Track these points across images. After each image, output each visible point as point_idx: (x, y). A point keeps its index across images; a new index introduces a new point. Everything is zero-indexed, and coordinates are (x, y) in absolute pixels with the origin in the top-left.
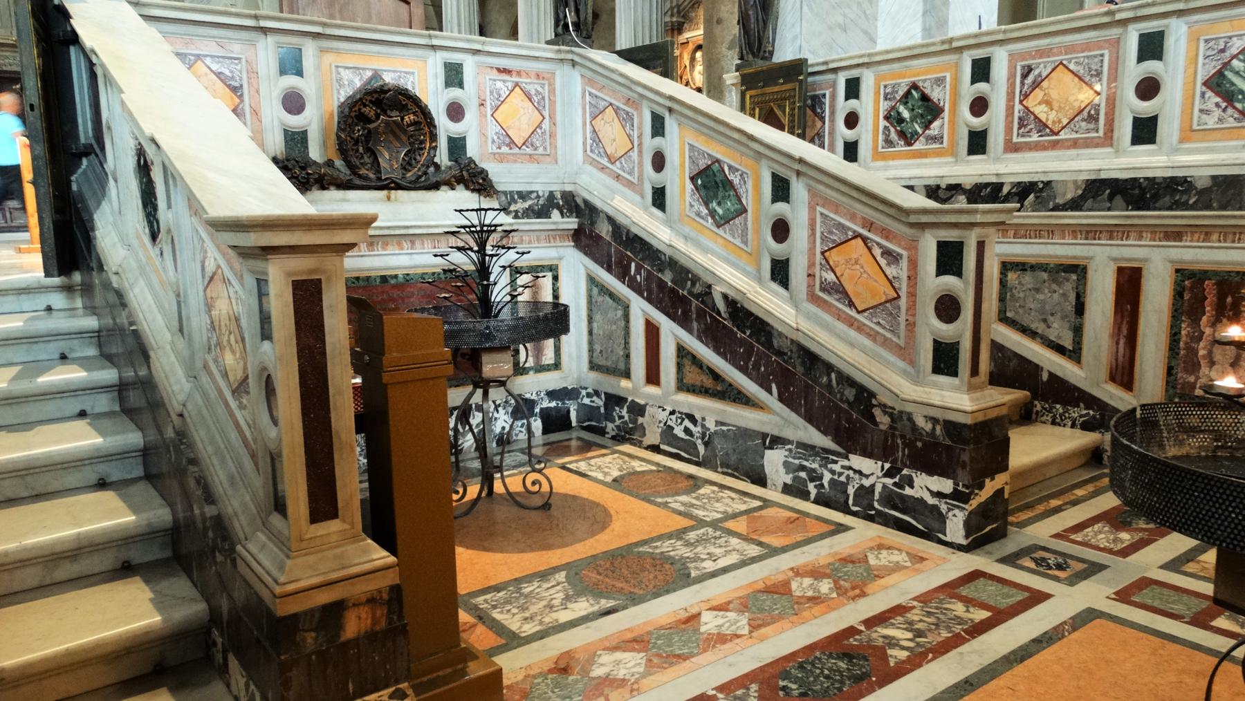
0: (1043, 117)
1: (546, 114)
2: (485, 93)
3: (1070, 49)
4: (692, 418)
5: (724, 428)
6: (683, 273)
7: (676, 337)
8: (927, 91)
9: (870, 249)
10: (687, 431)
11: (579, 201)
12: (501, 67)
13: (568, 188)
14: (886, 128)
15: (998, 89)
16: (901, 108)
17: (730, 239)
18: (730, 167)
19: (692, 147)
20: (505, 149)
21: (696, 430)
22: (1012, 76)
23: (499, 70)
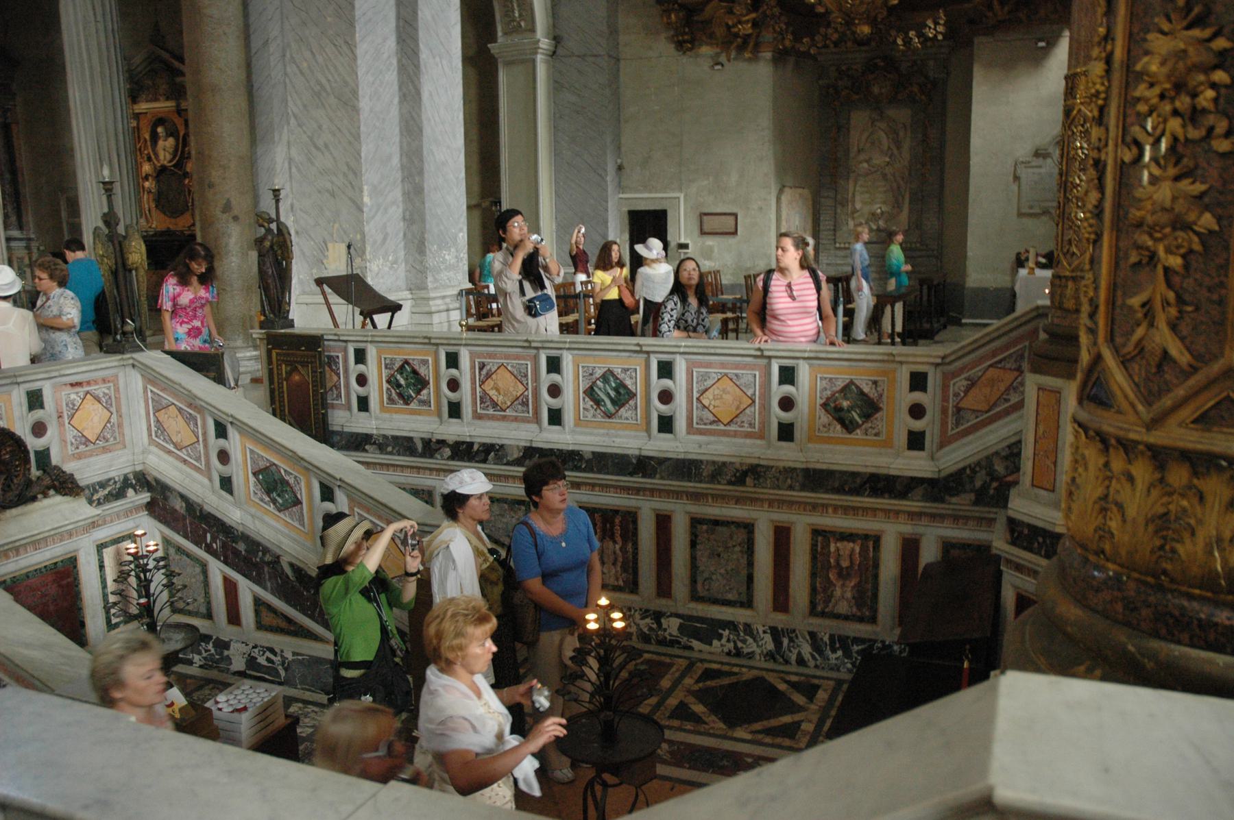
0: (495, 399)
1: (113, 410)
2: (61, 406)
3: (507, 357)
4: (272, 650)
5: (300, 658)
6: (254, 545)
7: (252, 591)
8: (417, 367)
10: (268, 660)
11: (149, 479)
12: (74, 382)
13: (138, 468)
14: (388, 389)
15: (465, 373)
16: (399, 377)
17: (290, 521)
18: (285, 471)
19: (252, 452)
20: (82, 448)
21: (277, 659)
22: (473, 367)
23: (72, 385)
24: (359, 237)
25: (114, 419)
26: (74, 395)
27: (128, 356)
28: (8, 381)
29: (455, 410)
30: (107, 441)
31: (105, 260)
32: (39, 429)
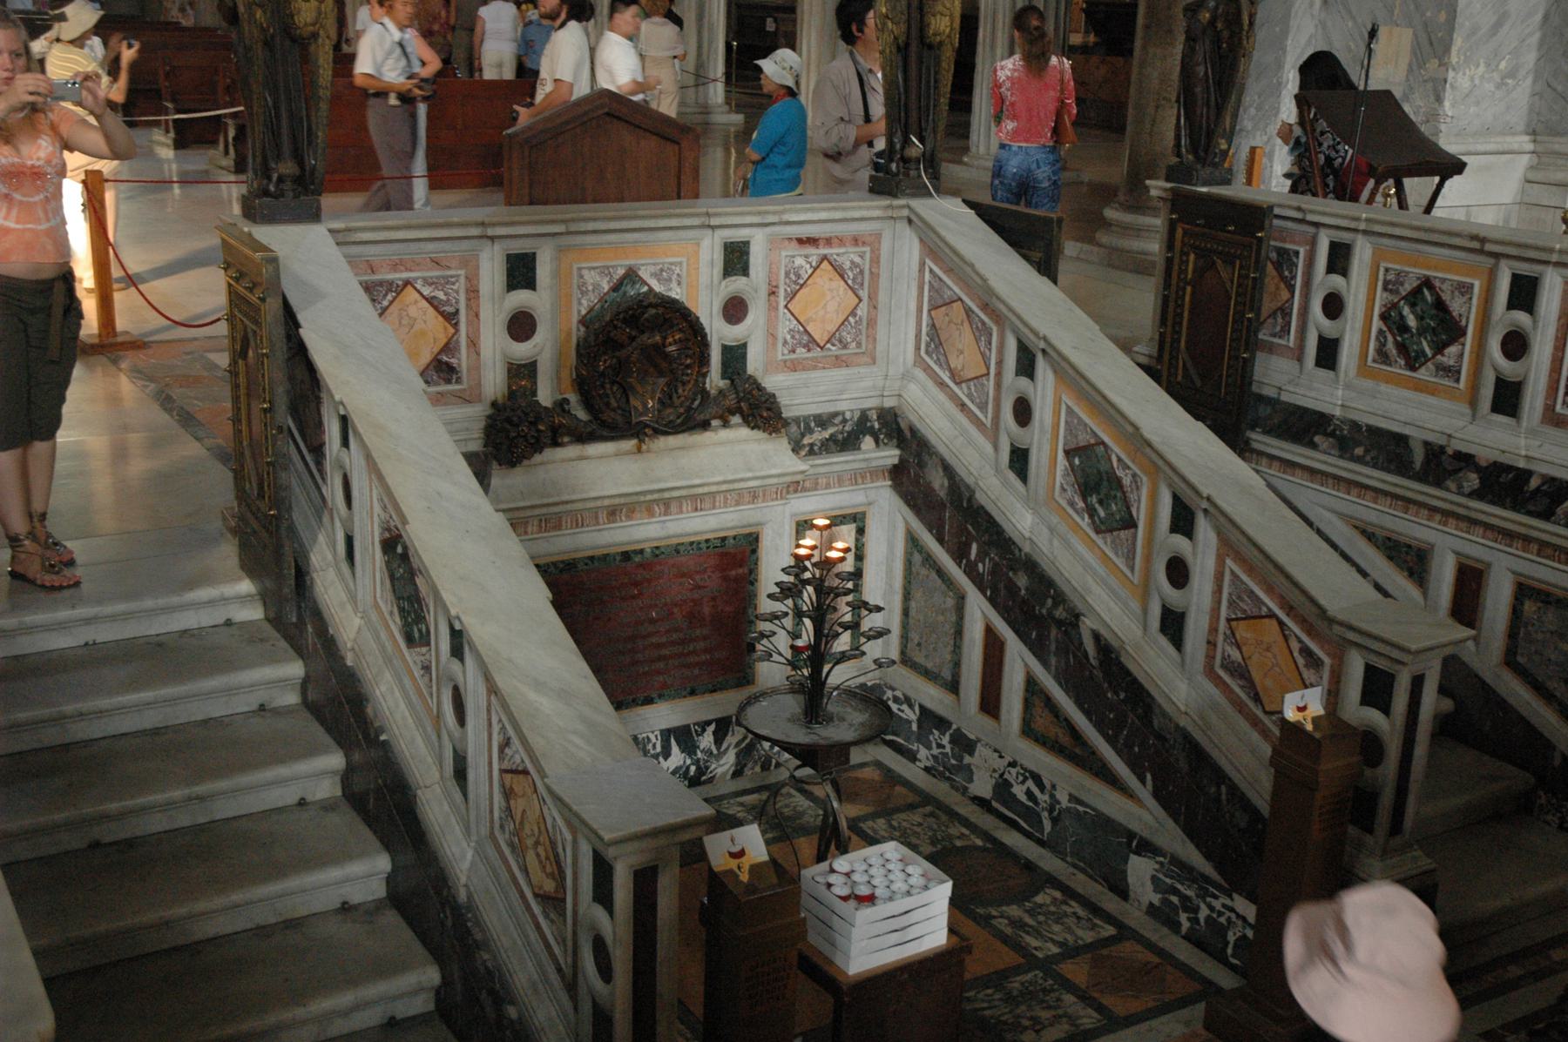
1: (864, 294)
2: (777, 275)
4: (1037, 779)
5: (1081, 809)
6: (1043, 583)
7: (1026, 665)
8: (1446, 297)
9: (1286, 638)
10: (1029, 794)
11: (903, 425)
12: (804, 236)
13: (889, 403)
14: (1380, 332)
16: (1406, 311)
17: (1111, 555)
18: (1119, 460)
19: (1070, 411)
20: (801, 351)
21: (1043, 798)
23: (800, 241)
24: (1443, 17)
25: (862, 311)
26: (802, 260)
27: (902, 202)
28: (696, 221)
29: (1507, 398)
30: (845, 347)
31: (890, 24)
32: (735, 310)
